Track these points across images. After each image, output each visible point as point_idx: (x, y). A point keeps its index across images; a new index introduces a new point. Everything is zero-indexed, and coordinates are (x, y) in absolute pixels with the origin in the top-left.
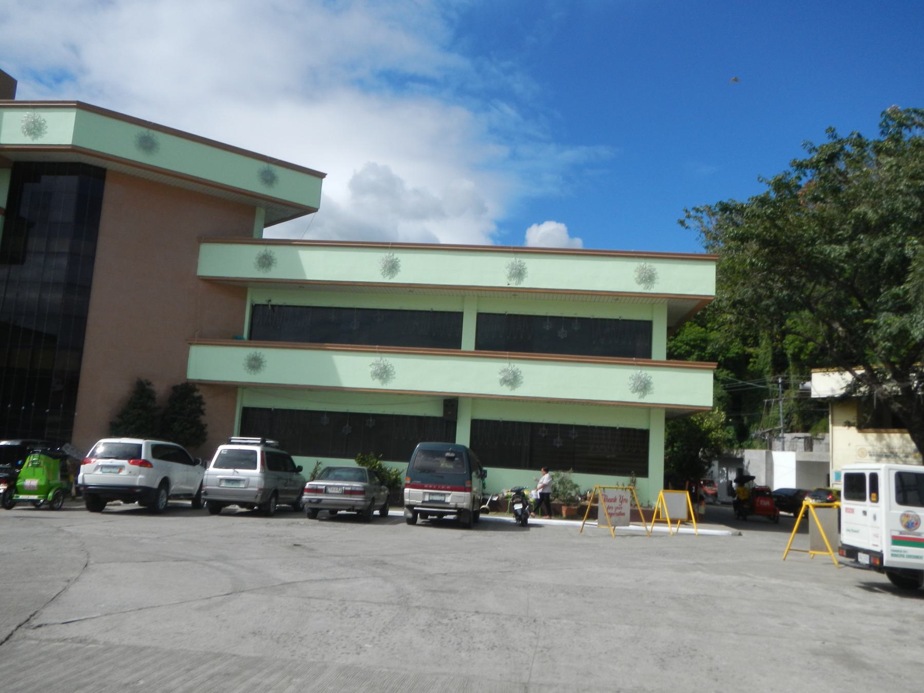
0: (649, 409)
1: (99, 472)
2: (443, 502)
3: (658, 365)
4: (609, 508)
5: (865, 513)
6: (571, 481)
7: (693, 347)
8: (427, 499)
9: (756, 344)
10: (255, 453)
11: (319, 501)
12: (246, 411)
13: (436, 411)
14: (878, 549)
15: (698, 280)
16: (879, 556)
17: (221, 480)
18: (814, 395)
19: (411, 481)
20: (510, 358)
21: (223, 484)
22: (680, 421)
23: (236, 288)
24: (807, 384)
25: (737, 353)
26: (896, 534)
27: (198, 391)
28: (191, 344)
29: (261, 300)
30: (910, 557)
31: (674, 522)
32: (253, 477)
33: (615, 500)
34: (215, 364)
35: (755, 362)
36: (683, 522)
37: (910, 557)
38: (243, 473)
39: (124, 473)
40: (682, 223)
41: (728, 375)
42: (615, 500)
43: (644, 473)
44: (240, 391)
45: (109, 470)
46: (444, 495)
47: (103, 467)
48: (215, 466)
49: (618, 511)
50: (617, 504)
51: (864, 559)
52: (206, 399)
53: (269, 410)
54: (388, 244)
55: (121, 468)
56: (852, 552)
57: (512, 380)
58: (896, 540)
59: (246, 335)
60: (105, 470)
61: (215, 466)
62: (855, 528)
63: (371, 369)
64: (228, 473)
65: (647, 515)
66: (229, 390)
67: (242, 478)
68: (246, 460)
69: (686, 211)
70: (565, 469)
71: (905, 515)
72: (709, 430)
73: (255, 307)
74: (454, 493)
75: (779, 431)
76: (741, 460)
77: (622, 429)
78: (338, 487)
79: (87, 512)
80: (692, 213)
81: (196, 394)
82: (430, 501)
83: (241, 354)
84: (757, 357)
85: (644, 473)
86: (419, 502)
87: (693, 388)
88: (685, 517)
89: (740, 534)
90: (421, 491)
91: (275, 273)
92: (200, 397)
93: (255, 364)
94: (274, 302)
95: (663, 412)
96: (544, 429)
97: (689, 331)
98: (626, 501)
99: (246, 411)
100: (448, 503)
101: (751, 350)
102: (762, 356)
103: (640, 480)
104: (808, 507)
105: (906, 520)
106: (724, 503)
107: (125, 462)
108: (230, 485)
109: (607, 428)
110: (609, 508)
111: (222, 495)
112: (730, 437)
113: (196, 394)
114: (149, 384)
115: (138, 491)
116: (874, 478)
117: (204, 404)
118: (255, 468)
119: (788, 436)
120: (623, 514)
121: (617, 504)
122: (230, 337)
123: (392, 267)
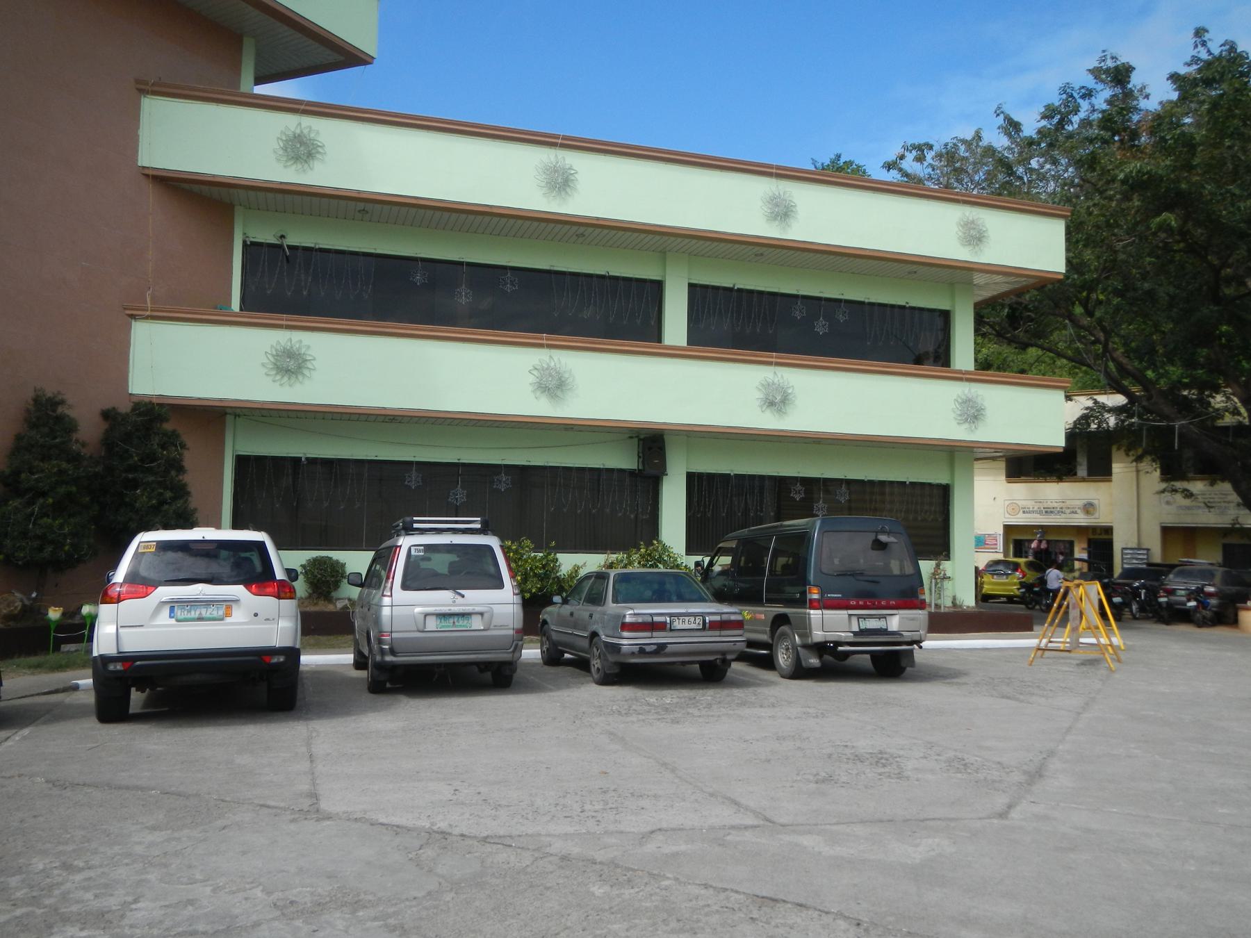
1: (164, 618)
2: (884, 632)
8: (856, 629)
10: (489, 549)
11: (662, 647)
12: (242, 462)
13: (623, 459)
15: (1033, 245)
17: (426, 615)
19: (822, 594)
20: (778, 364)
21: (432, 624)
23: (207, 201)
27: (167, 420)
28: (133, 317)
29: (266, 236)
32: (499, 604)
34: (194, 360)
38: (476, 598)
39: (238, 615)
44: (229, 419)
45: (194, 614)
46: (884, 617)
47: (173, 605)
48: (405, 586)
52: (187, 439)
53: (296, 461)
54: (557, 137)
55: (229, 604)
57: (777, 401)
59: (236, 305)
60: (179, 613)
61: (405, 586)
63: (532, 379)
64: (442, 599)
66: (212, 417)
67: (478, 609)
68: (471, 569)
73: (251, 249)
74: (901, 612)
78: (695, 615)
79: (92, 723)
81: (168, 427)
82: (862, 632)
83: (262, 341)
86: (849, 637)
90: (843, 613)
91: (322, 175)
92: (174, 435)
93: (290, 365)
94: (294, 239)
96: (799, 487)
97: (1021, 326)
99: (242, 462)
100: (893, 633)
103: (946, 565)
107: (238, 590)
108: (448, 624)
111: (440, 652)
113: (168, 427)
114: (62, 402)
115: (275, 660)
117: (183, 446)
118: (500, 585)
122: (200, 307)
123: (561, 182)
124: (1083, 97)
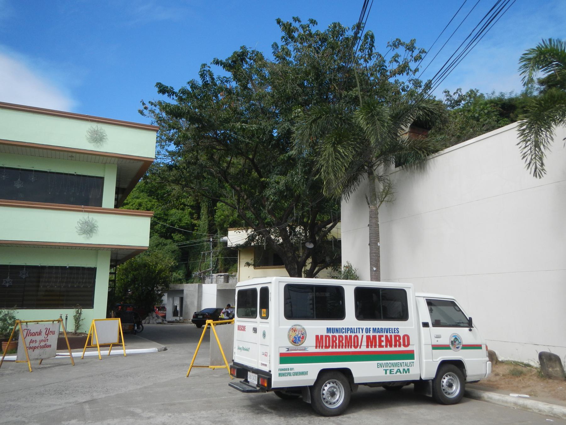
0: (96, 250)
3: (107, 212)
4: (32, 341)
5: (255, 330)
6: (13, 318)
7: (159, 219)
9: (199, 218)
14: (266, 369)
15: (142, 145)
16: (265, 376)
18: (229, 244)
22: (119, 257)
24: (225, 238)
25: (187, 223)
26: (284, 351)
30: (296, 374)
31: (104, 346)
33: (40, 333)
35: (197, 230)
36: (114, 345)
37: (296, 374)
40: (141, 112)
41: (180, 237)
42: (40, 333)
43: (90, 304)
49: (43, 344)
50: (42, 337)
51: (253, 379)
56: (241, 371)
58: (285, 358)
62: (246, 346)
65: (78, 341)
69: (144, 104)
70: (10, 306)
71: (293, 330)
72: (161, 271)
75: (209, 271)
76: (182, 291)
77: (71, 268)
80: (148, 105)
84: (199, 226)
85: (90, 304)
87: (132, 231)
88: (116, 341)
89: (165, 349)
95: (109, 252)
98: (53, 333)
101: (196, 222)
102: (202, 226)
104: (209, 324)
105: (293, 335)
106: (169, 322)
109: (57, 268)
110: (32, 341)
112: (181, 277)
116: (265, 291)
119: (215, 275)
120: (50, 346)
121: (42, 337)
124: (227, 81)
